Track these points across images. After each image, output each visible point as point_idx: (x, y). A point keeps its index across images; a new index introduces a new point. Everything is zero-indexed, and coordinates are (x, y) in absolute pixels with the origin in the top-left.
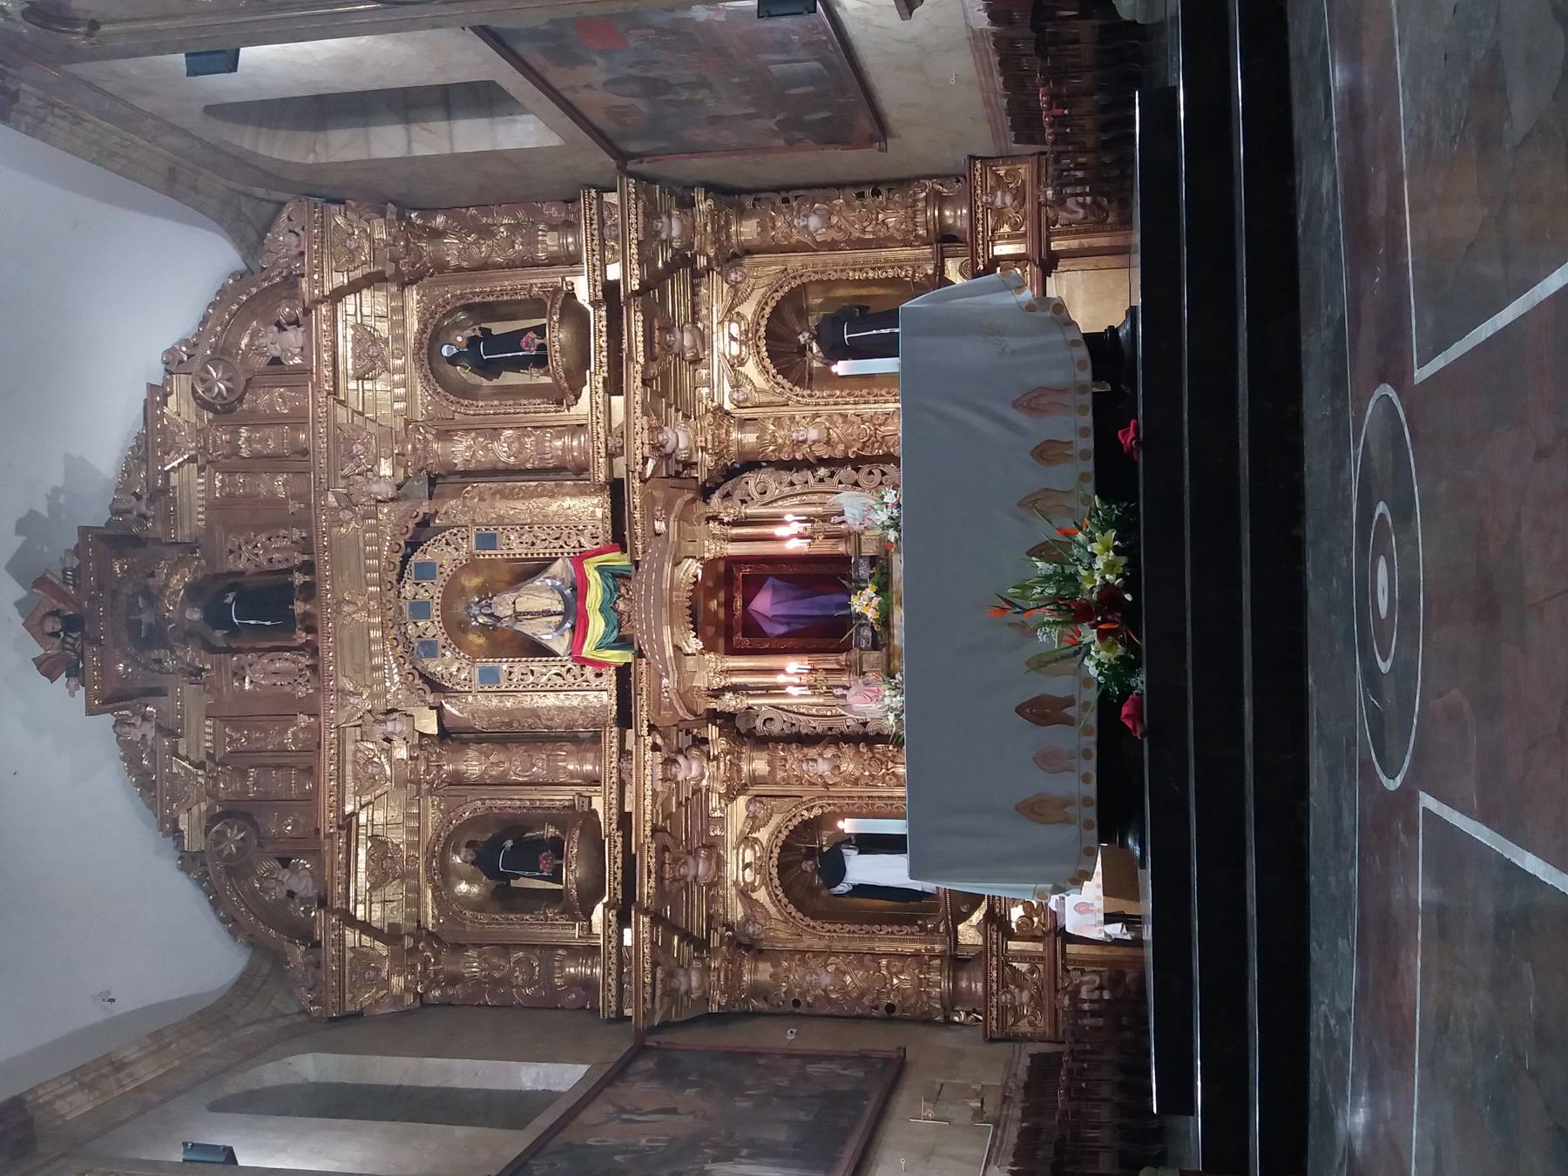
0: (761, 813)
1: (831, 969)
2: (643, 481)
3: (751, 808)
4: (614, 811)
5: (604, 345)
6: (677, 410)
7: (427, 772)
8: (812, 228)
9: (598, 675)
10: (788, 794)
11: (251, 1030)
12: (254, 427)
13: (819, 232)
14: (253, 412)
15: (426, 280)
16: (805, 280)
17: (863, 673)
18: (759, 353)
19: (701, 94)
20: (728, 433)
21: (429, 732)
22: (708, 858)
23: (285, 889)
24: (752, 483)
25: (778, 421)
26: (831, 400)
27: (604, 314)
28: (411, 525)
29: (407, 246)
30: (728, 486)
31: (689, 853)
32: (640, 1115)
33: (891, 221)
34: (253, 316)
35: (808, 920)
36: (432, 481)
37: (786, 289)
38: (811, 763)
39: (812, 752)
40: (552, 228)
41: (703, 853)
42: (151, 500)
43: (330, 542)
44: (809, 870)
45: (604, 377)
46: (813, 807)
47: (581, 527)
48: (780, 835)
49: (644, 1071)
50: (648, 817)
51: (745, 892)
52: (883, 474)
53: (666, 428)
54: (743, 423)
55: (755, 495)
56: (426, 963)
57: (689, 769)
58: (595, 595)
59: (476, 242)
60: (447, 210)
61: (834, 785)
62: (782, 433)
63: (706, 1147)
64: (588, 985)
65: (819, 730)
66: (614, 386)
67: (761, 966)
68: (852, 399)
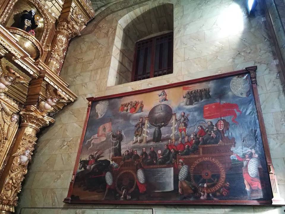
8: (22, 157)
29: (69, 29)
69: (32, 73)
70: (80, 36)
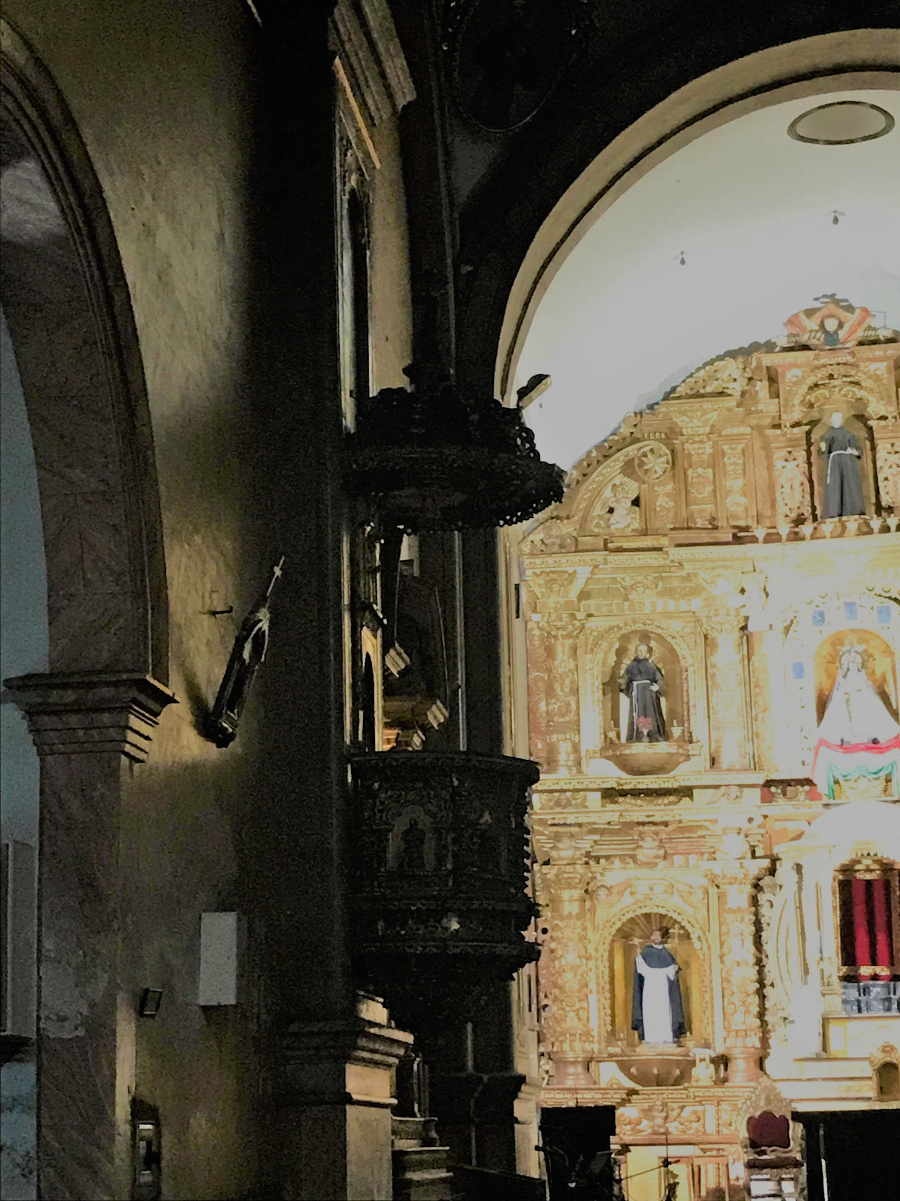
22: (657, 857)
31: (661, 841)
41: (662, 852)
56: (563, 628)
65: (765, 947)
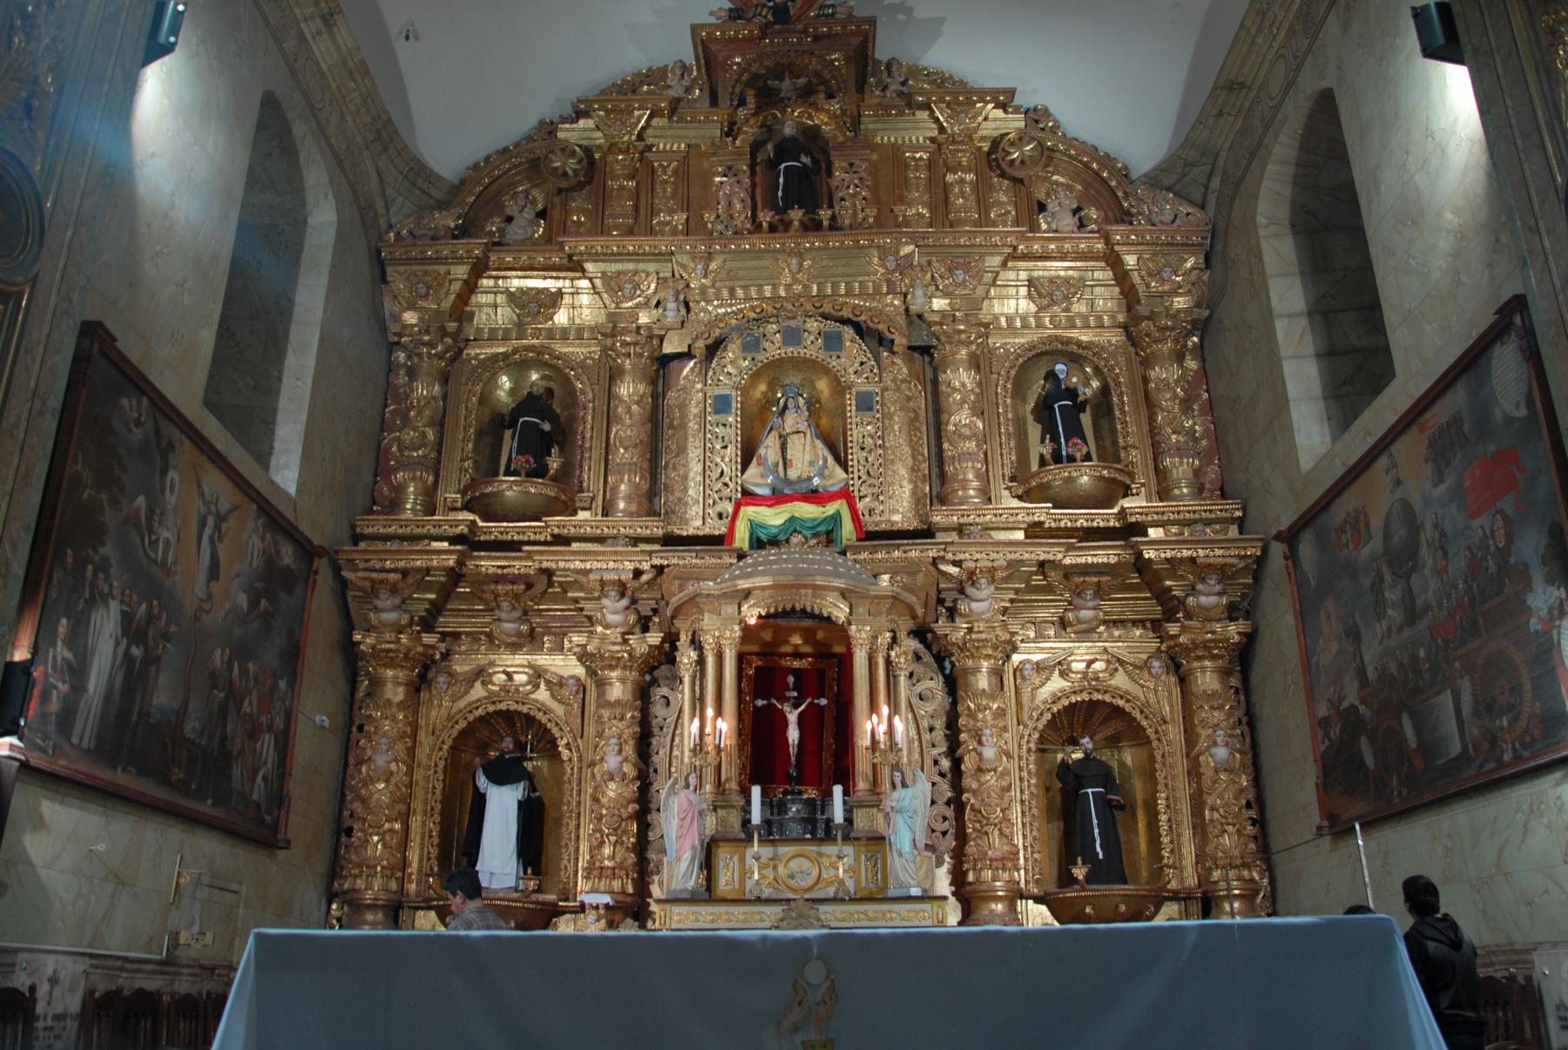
0: (566, 692)
1: (393, 767)
2: (935, 562)
3: (571, 681)
4: (573, 530)
5: (1078, 524)
6: (1012, 601)
7: (625, 344)
9: (720, 516)
10: (586, 723)
11: (373, 174)
12: (976, 186)
13: (1210, 759)
14: (991, 187)
15: (1132, 349)
16: (1155, 743)
17: (715, 809)
18: (1075, 692)
19: (1395, 615)
20: (988, 657)
21: (665, 344)
22: (519, 634)
23: (515, 214)
24: (931, 684)
25: (1001, 713)
26: (1025, 774)
27: (1111, 524)
28: (881, 327)
29: (1166, 328)
30: (928, 658)
31: (525, 613)
32: (211, 538)
33: (1226, 840)
34: (1087, 186)
35: (449, 742)
36: (926, 350)
37: (1144, 723)
38: (617, 748)
39: (629, 750)
40: (1197, 473)
41: (524, 628)
42: (901, 94)
43: (863, 247)
44: (504, 744)
45: (1043, 523)
46: (570, 750)
47: (881, 498)
48: (541, 714)
49: (278, 552)
50: (562, 565)
51: (481, 674)
52: (944, 833)
53: (992, 588)
54: (998, 674)
55: (919, 688)
56: (430, 344)
57: (613, 611)
58: (808, 511)
59: (1175, 395)
60: (1203, 371)
61: (593, 775)
62: (989, 718)
63: (150, 607)
64: (395, 505)
65: (655, 759)
66: (1035, 531)
67: (401, 690)
68: (1026, 797)
69: (1113, 560)
70: (1211, 315)
